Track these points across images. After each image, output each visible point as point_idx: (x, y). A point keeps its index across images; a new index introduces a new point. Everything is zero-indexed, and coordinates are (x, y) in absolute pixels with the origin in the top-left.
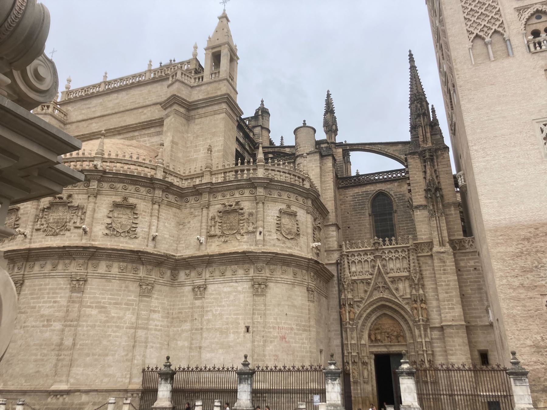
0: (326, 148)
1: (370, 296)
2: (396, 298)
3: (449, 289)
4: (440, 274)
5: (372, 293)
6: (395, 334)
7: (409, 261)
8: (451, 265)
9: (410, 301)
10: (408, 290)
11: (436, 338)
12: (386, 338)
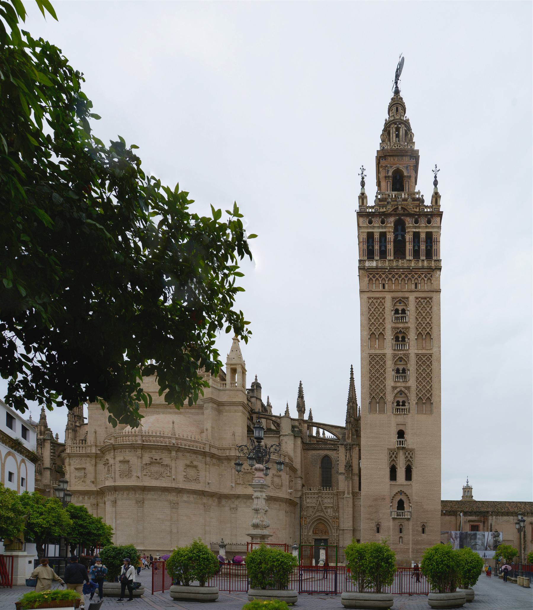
0: (297, 431)
1: (315, 514)
5: (315, 513)
10: (332, 513)
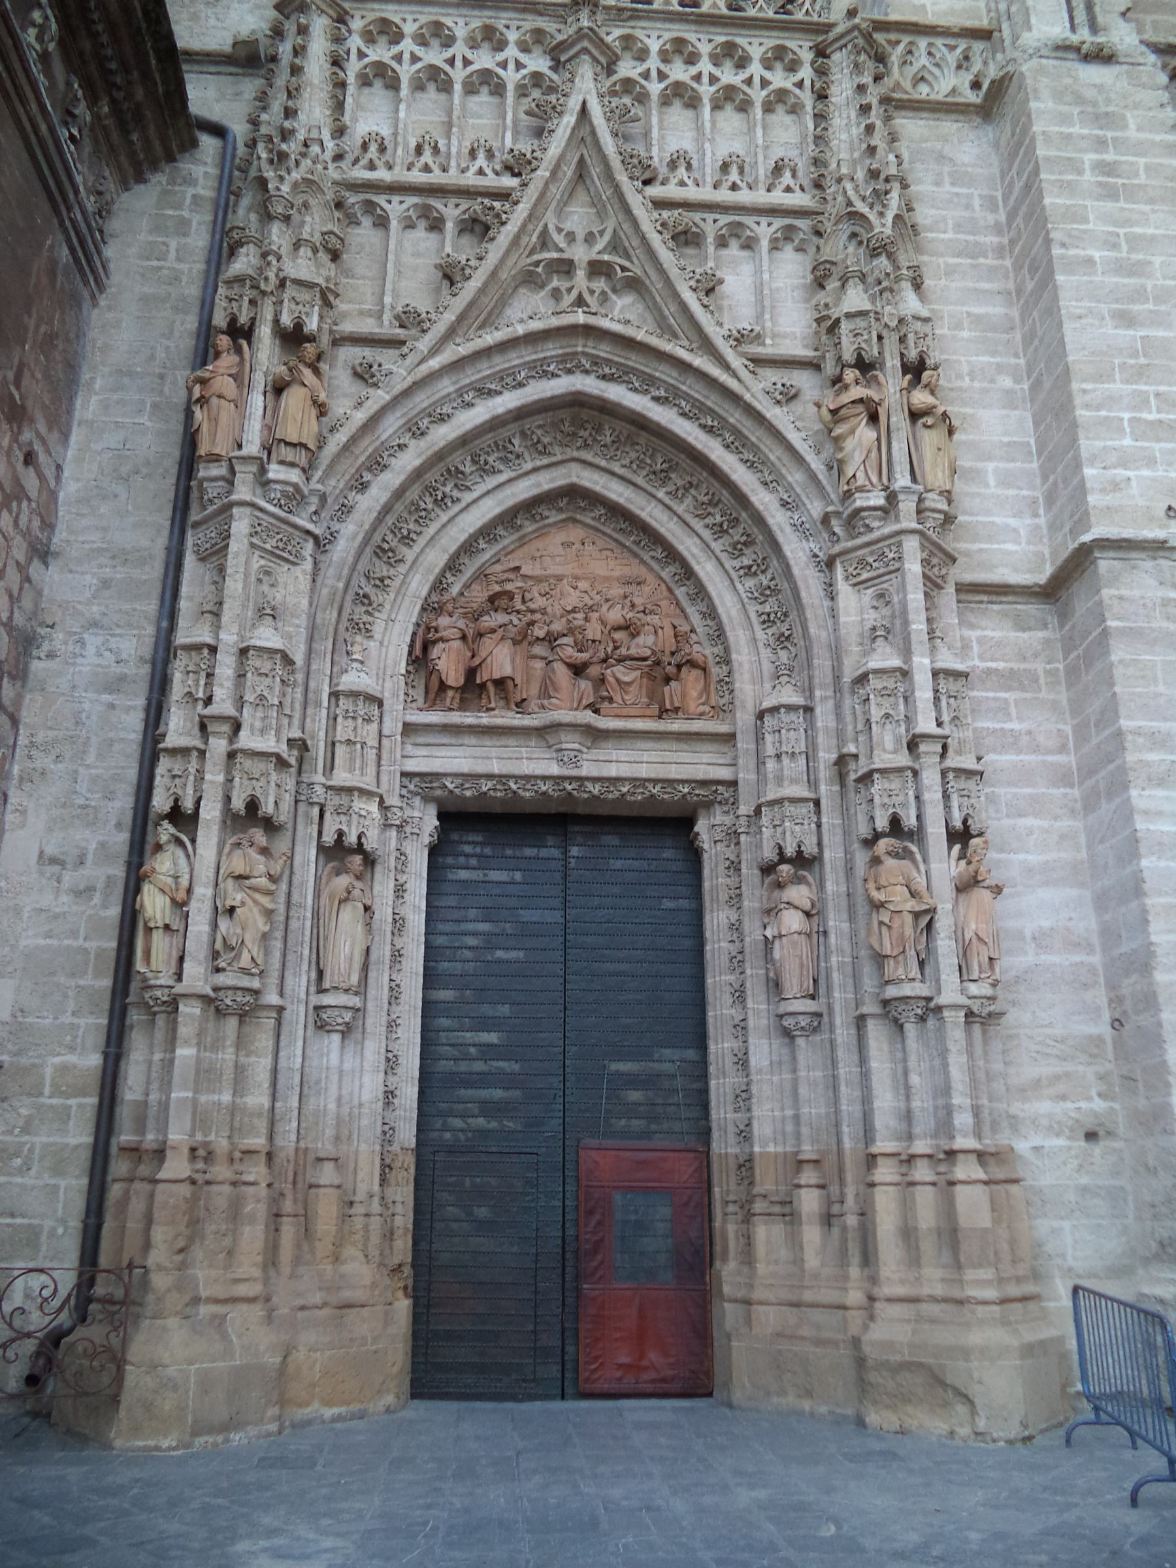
2: (707, 346)
3: (1140, 295)
4: (1069, 188)
6: (643, 644)
7: (820, 117)
8: (1153, 144)
9: (802, 380)
11: (989, 672)
12: (562, 673)
